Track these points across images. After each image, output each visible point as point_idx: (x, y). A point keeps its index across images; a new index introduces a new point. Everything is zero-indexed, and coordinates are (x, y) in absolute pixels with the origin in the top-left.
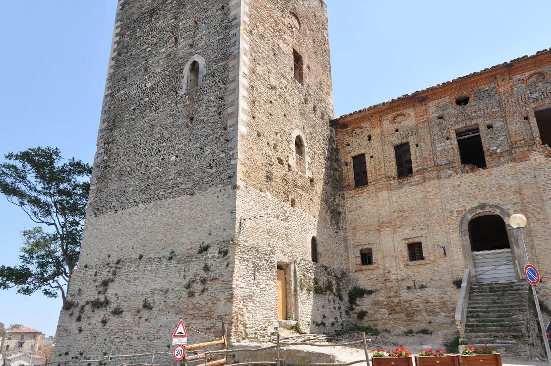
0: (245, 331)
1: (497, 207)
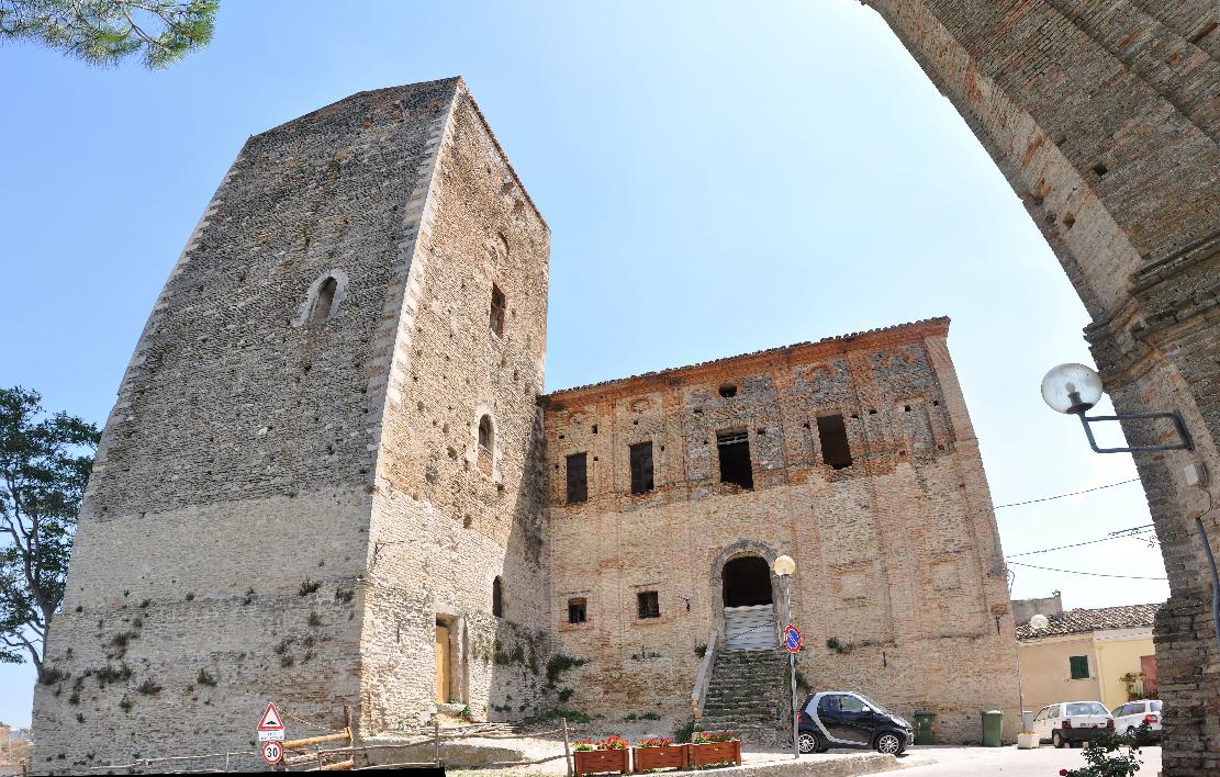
0: (383, 720)
1: (762, 546)
